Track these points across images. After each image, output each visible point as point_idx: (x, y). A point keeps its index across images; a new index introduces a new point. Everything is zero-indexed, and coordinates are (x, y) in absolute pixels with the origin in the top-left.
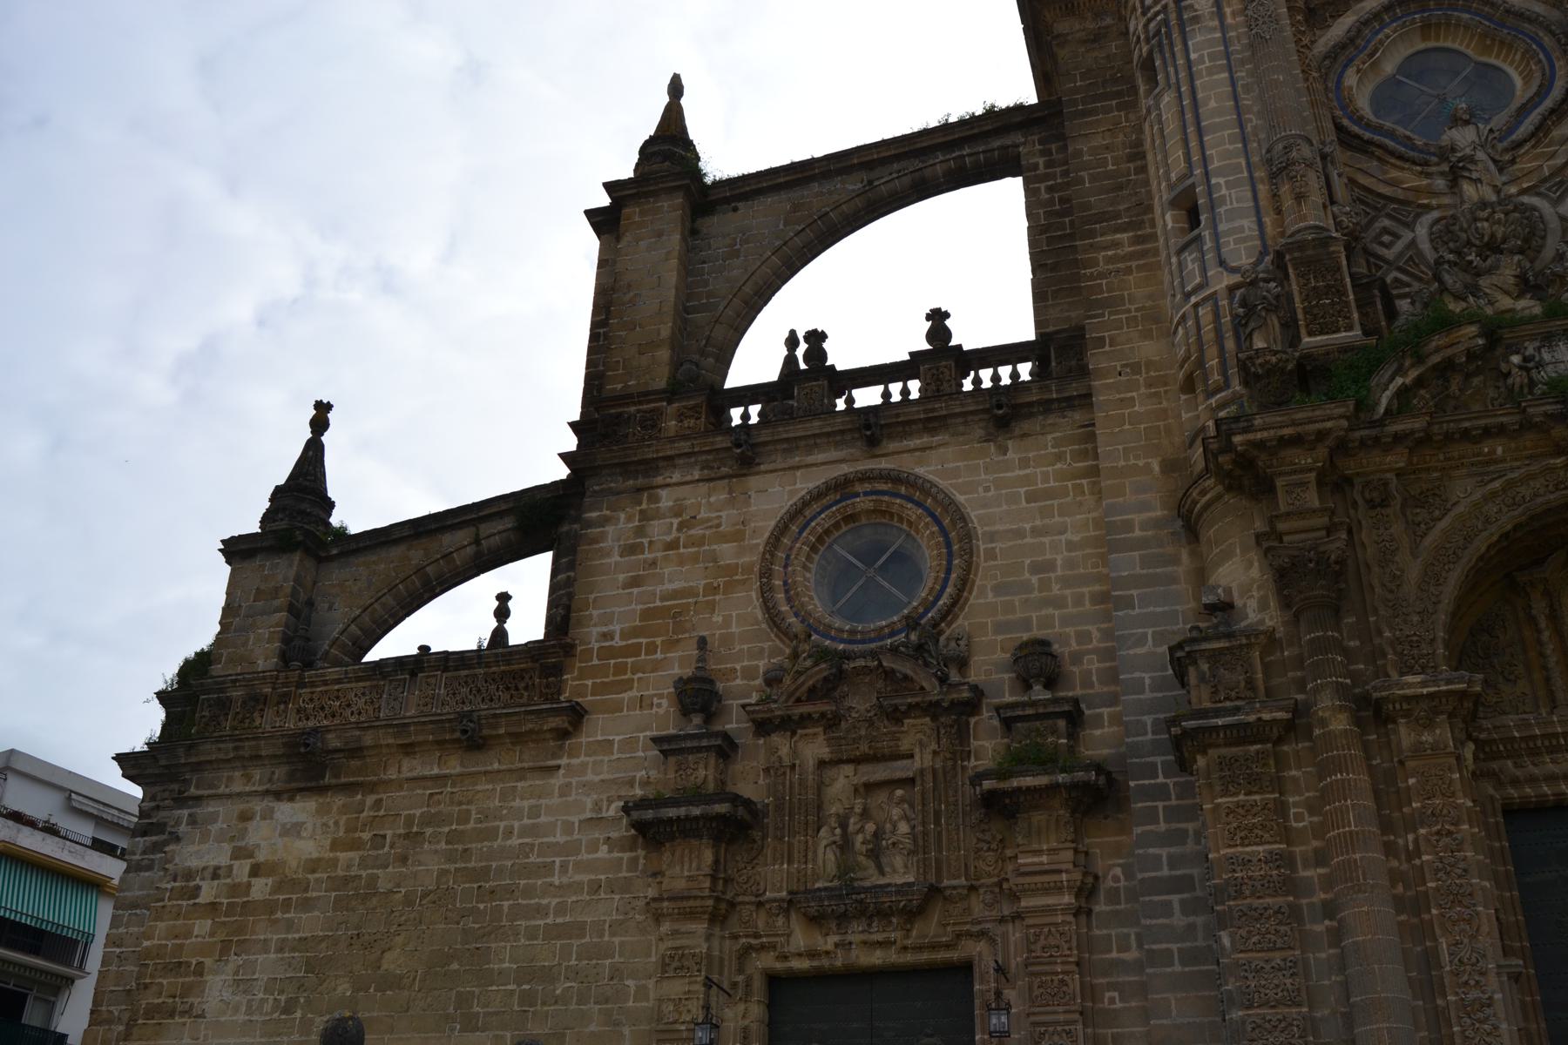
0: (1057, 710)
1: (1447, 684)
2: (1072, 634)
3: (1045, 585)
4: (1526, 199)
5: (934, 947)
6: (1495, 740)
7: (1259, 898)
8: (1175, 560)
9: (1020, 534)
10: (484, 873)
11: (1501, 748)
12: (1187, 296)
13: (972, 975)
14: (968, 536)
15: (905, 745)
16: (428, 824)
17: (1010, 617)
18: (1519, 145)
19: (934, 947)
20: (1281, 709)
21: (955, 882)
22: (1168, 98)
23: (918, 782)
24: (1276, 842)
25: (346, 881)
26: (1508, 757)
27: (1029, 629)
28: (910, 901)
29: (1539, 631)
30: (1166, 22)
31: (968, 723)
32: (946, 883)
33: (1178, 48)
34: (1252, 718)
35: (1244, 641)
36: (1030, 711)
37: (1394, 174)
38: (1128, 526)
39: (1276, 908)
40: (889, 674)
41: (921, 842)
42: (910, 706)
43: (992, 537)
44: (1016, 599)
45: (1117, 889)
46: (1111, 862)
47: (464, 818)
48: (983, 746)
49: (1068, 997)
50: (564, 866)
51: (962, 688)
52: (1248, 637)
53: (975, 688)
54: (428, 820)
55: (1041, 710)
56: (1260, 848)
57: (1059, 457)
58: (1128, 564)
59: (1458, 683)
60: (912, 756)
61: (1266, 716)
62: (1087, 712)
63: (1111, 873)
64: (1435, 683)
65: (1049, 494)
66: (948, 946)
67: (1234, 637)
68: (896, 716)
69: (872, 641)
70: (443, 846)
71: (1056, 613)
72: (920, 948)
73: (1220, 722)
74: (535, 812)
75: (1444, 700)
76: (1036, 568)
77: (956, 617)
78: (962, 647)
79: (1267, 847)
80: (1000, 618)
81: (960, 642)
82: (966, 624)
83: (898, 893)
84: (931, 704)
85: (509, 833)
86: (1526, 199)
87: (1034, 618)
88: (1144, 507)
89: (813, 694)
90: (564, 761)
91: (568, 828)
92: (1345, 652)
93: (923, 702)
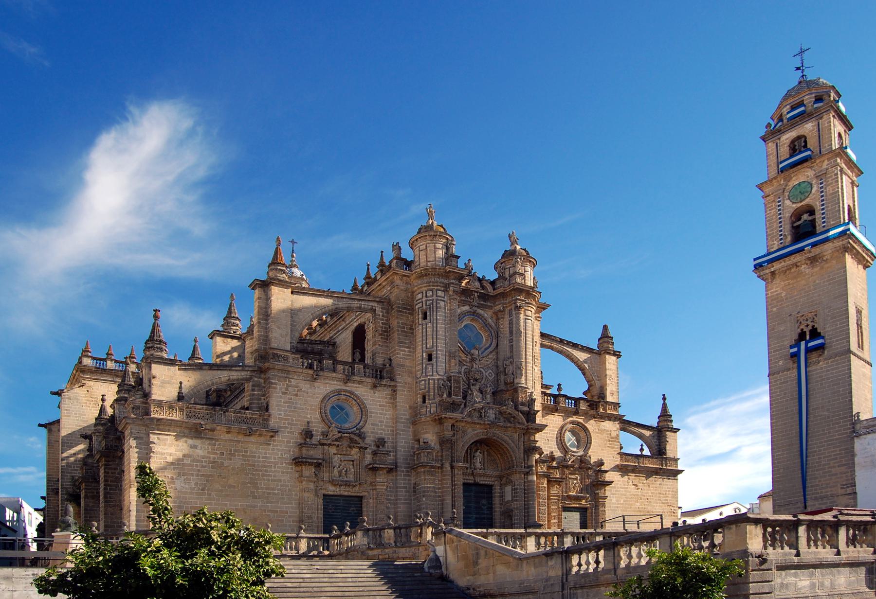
3: (381, 426)
4: (481, 369)
8: (410, 428)
9: (377, 413)
10: (254, 465)
12: (427, 376)
14: (367, 412)
16: (236, 452)
18: (483, 357)
22: (429, 325)
25: (214, 462)
30: (433, 303)
33: (435, 313)
37: (460, 355)
38: (402, 418)
40: (350, 439)
43: (371, 412)
44: (376, 427)
47: (246, 452)
50: (275, 467)
54: (235, 451)
57: (386, 398)
58: (401, 426)
65: (383, 406)
68: (351, 447)
70: (241, 457)
74: (265, 453)
76: (380, 422)
85: (259, 457)
86: (481, 369)
88: (405, 415)
89: (336, 440)
90: (272, 443)
91: (275, 458)
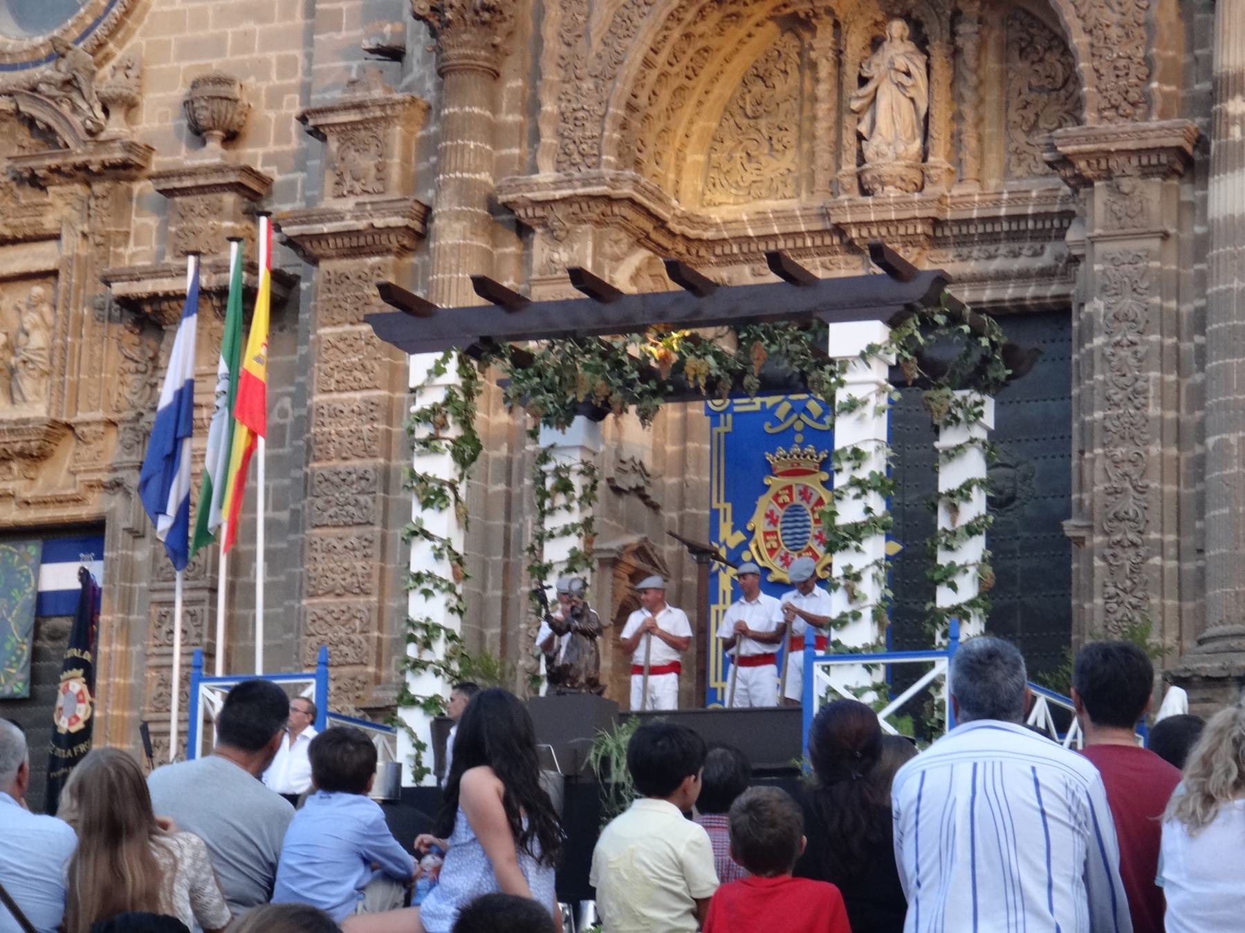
0: (221, 181)
1: (584, 185)
2: (274, 61)
5: (60, 501)
6: (724, 240)
7: (345, 459)
11: (735, 250)
13: (102, 537)
15: (49, 222)
17: (201, 34)
19: (60, 501)
20: (396, 214)
21: (89, 416)
23: (62, 275)
24: (376, 388)
26: (747, 261)
27: (221, 53)
28: (29, 441)
29: (817, 81)
31: (130, 191)
32: (81, 416)
34: (362, 225)
35: (378, 113)
36: (188, 183)
39: (361, 472)
41: (57, 362)
42: (57, 170)
45: (282, 427)
46: (279, 390)
48: (146, 225)
49: (197, 569)
51: (112, 145)
52: (383, 107)
53: (130, 147)
55: (202, 181)
56: (358, 395)
59: (598, 184)
60: (56, 237)
61: (379, 223)
62: (277, 178)
63: (278, 406)
64: (570, 182)
66: (77, 501)
67: (366, 107)
68: (36, 182)
69: (24, 66)
71: (258, 28)
72: (43, 503)
73: (326, 228)
75: (584, 206)
77: (130, 32)
78: (133, 81)
79: (366, 394)
80: (188, 34)
81: (129, 72)
82: (144, 43)
83: (11, 431)
84: (77, 168)
87: (230, 36)
92: (494, 133)
93: (65, 165)
